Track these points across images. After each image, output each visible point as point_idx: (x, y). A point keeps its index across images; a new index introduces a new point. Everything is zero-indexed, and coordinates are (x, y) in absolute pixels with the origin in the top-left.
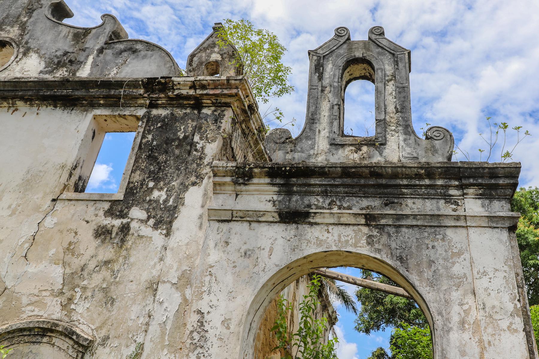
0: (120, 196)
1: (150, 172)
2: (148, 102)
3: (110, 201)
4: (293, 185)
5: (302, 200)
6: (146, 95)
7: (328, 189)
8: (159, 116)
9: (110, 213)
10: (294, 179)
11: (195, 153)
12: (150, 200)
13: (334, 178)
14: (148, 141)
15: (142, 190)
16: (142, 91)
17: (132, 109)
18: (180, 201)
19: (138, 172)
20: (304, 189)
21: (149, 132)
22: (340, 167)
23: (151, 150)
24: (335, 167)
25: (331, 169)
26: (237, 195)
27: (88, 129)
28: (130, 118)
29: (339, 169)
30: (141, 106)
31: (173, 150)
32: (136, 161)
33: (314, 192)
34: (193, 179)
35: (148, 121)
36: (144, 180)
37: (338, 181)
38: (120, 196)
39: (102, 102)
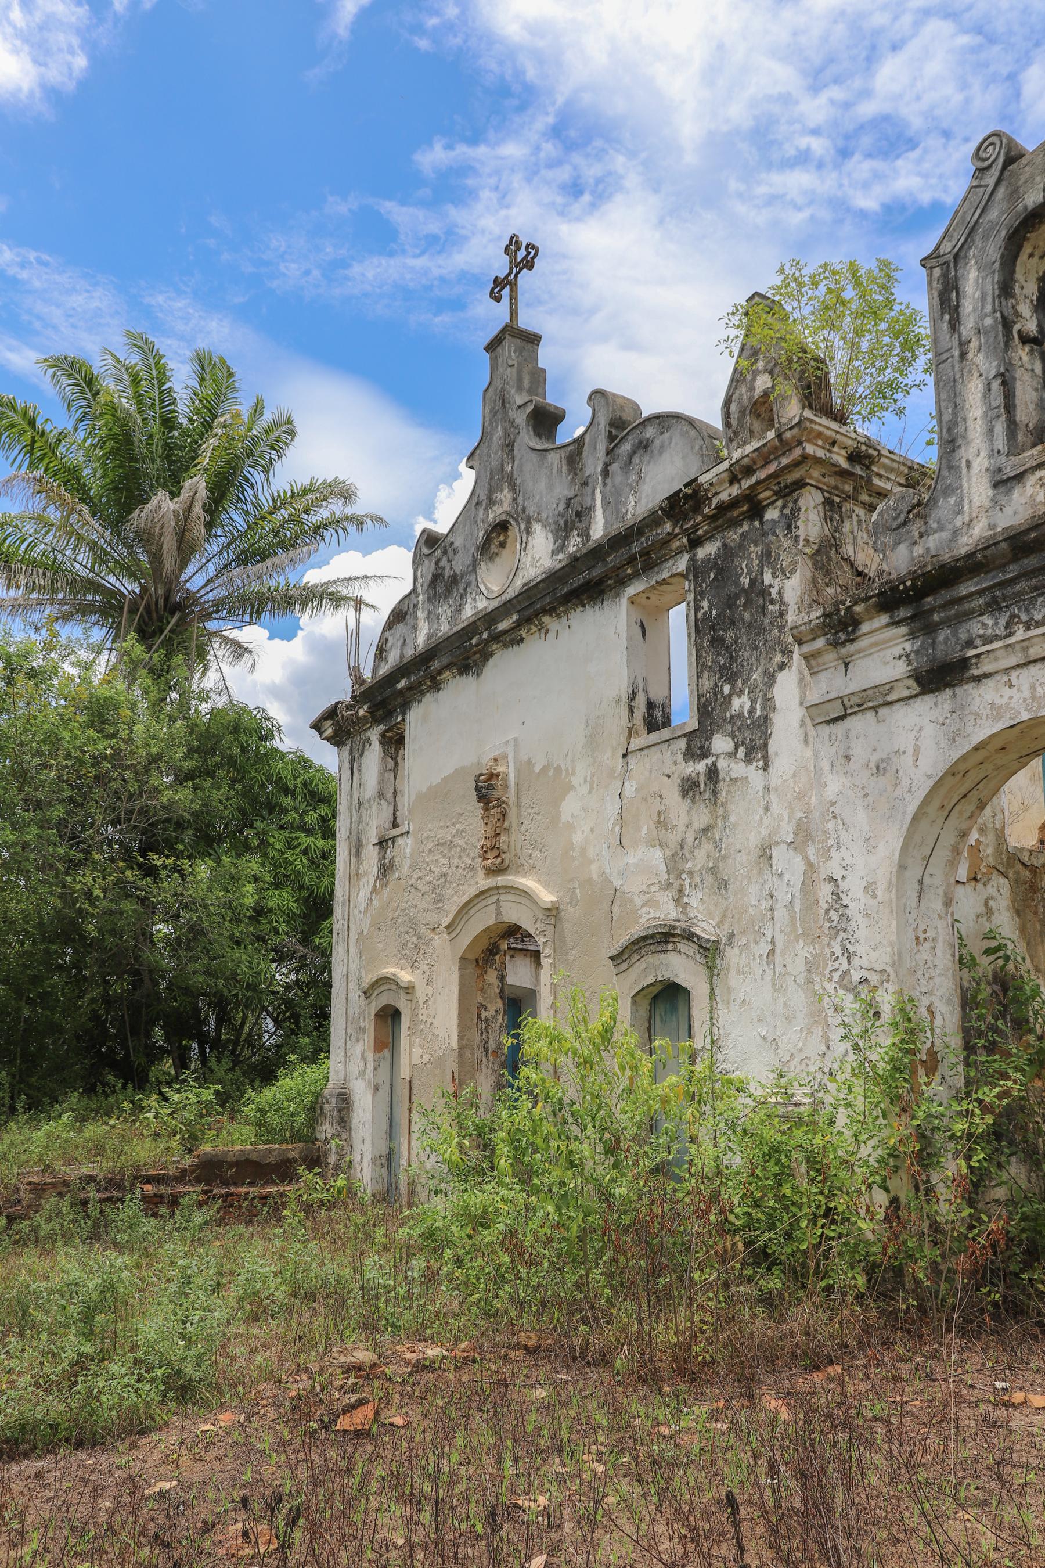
0: (694, 725)
1: (722, 668)
2: (685, 540)
3: (685, 735)
4: (931, 611)
5: (955, 634)
6: (677, 530)
7: (998, 594)
8: (707, 559)
9: (690, 754)
10: (929, 599)
11: (771, 607)
12: (732, 717)
13: (1002, 567)
14: (705, 613)
15: (718, 703)
16: (668, 527)
17: (671, 562)
18: (769, 703)
19: (706, 675)
20: (953, 612)
21: (702, 594)
22: (1005, 540)
23: (713, 628)
24: (995, 544)
25: (988, 552)
26: (846, 665)
27: (628, 626)
28: (674, 580)
29: (1004, 545)
30: (680, 552)
31: (740, 614)
32: (698, 657)
33: (973, 611)
34: (778, 658)
35: (696, 577)
36: (716, 685)
37: (1012, 571)
38: (694, 725)
39: (629, 571)
